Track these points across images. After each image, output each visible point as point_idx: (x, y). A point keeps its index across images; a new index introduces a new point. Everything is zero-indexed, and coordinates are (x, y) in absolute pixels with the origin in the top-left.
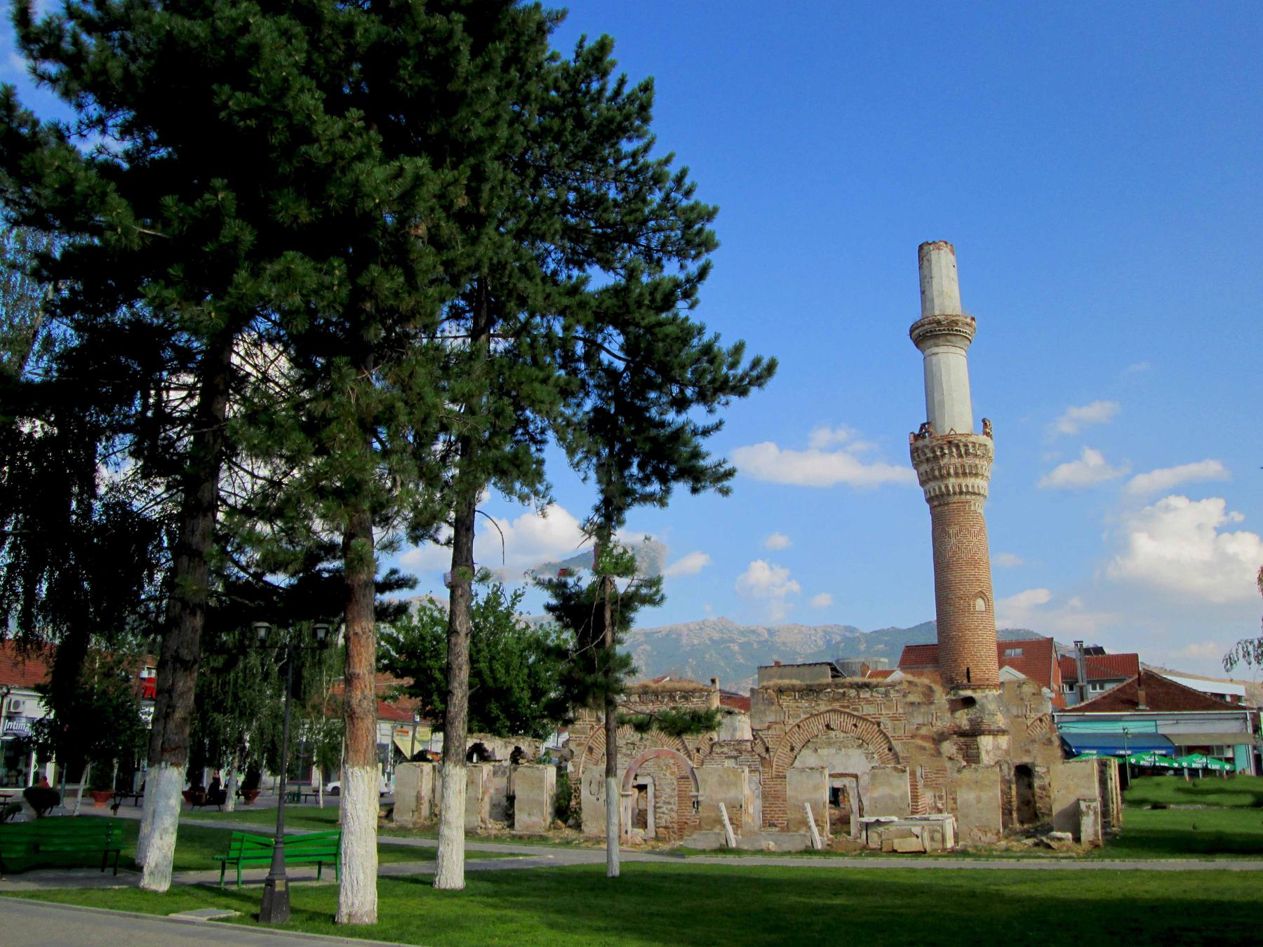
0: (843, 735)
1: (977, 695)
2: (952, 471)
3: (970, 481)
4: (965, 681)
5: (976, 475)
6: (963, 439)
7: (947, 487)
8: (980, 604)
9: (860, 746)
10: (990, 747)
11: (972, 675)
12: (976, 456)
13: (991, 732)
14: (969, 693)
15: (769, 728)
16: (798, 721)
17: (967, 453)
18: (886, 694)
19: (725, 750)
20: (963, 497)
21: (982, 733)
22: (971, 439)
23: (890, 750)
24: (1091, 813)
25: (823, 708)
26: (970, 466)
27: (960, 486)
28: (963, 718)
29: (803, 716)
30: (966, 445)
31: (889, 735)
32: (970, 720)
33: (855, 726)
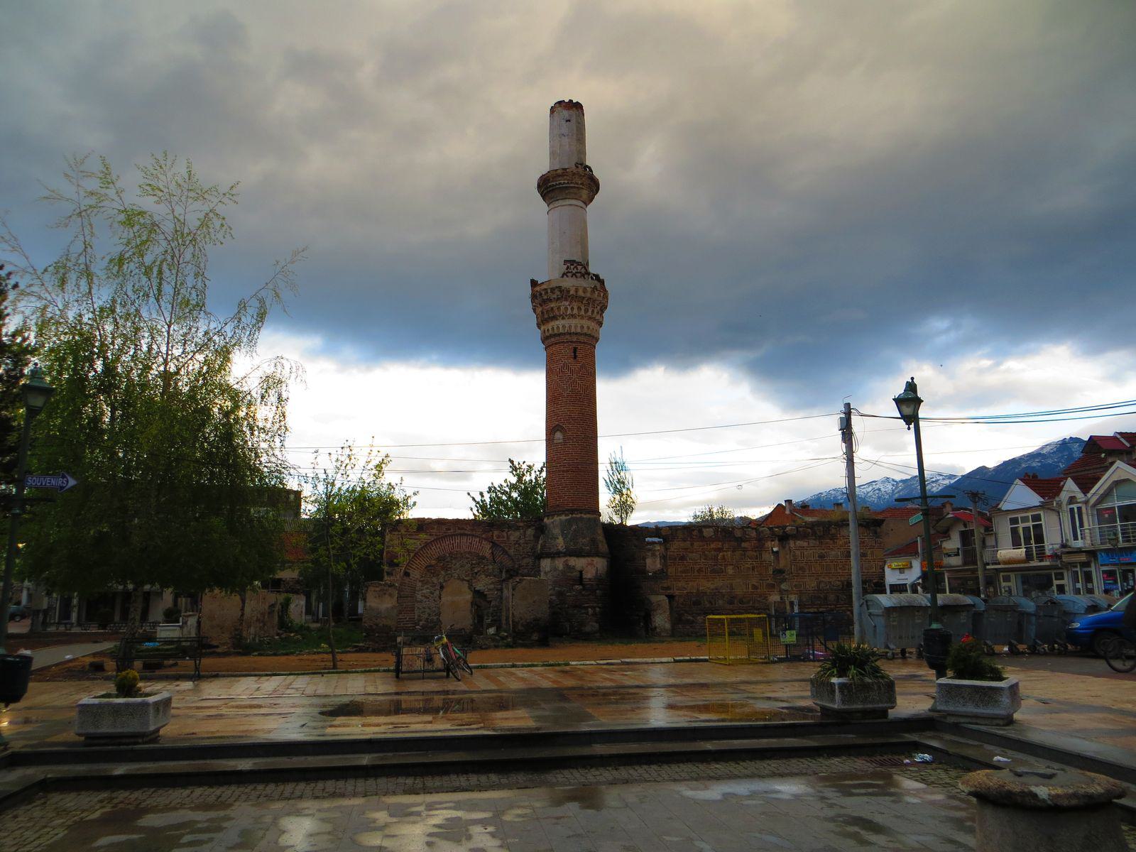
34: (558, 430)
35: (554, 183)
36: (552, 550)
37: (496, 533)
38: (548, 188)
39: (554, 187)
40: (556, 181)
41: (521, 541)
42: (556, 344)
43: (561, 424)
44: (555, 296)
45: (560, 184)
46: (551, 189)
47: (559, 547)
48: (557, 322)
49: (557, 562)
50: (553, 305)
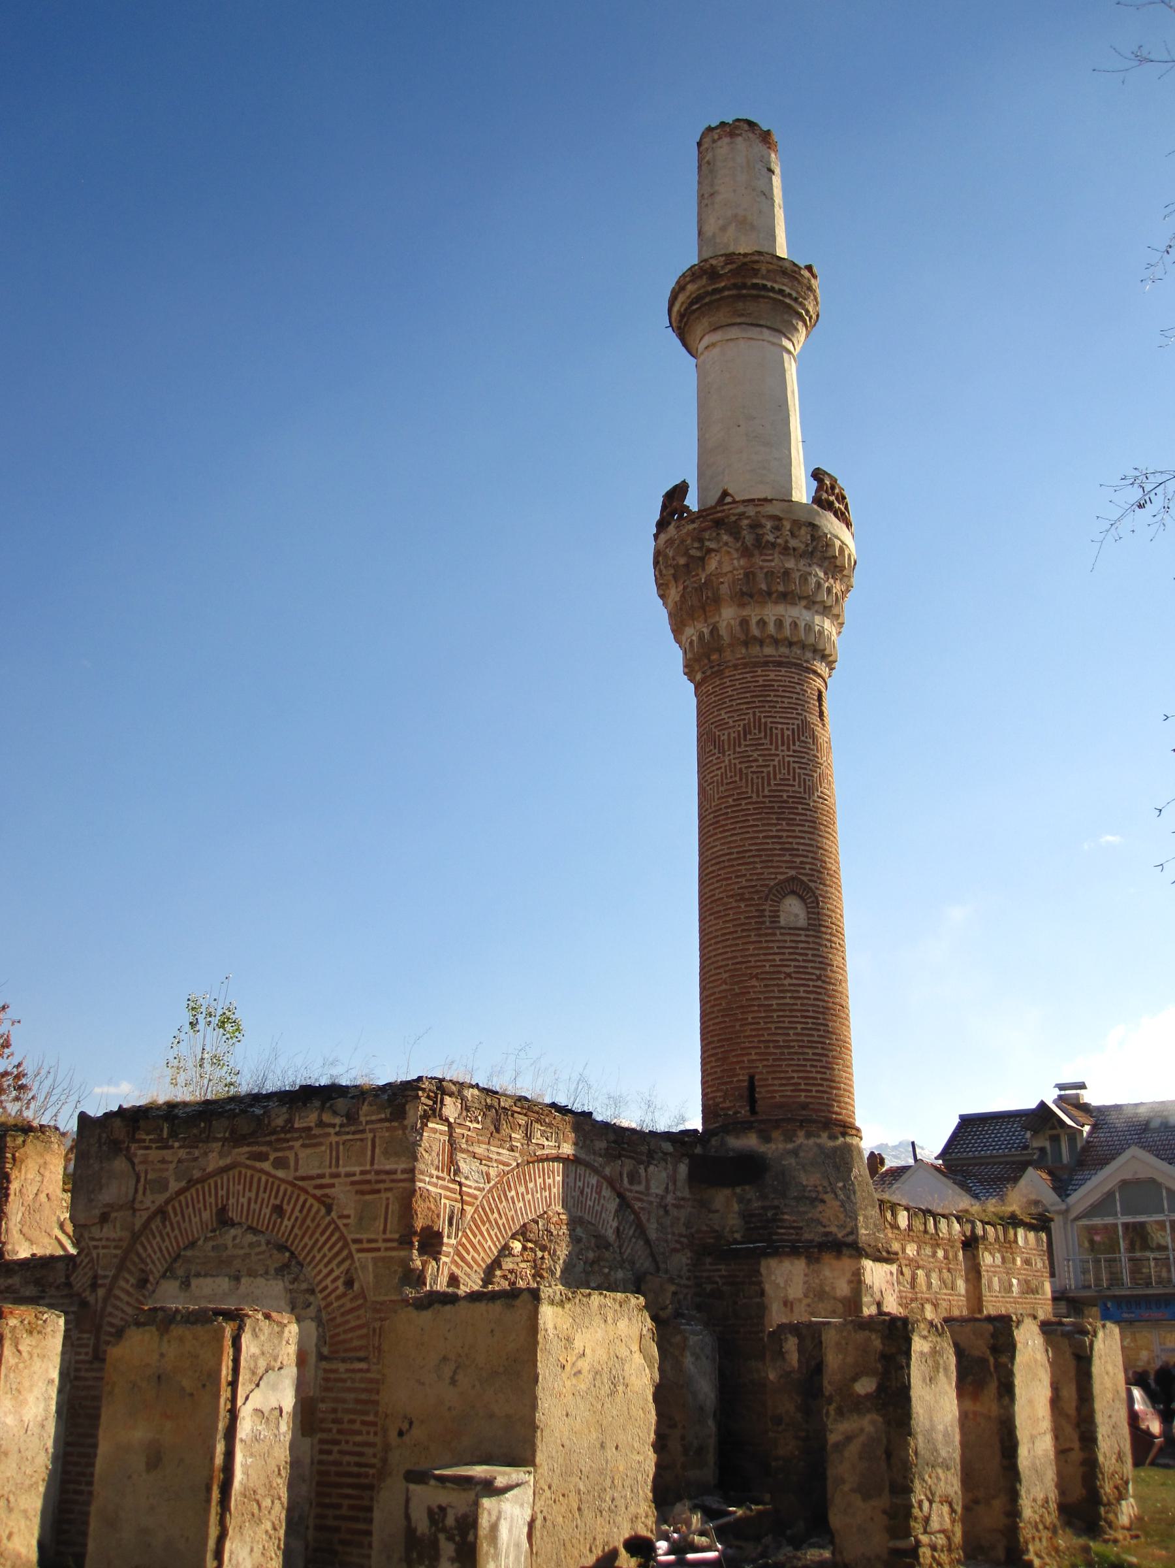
0: (250, 1238)
1: (774, 1148)
2: (724, 589)
3: (772, 612)
4: (744, 1112)
5: (786, 597)
6: (751, 511)
7: (714, 630)
8: (793, 910)
9: (282, 1270)
10: (796, 1291)
11: (760, 1093)
12: (786, 550)
13: (795, 1250)
14: (750, 1142)
15: (104, 1218)
16: (161, 1199)
17: (761, 545)
18: (352, 1117)
19: (15, 1280)
20: (755, 650)
21: (775, 1251)
22: (770, 509)
23: (349, 1283)
24: (447, 1549)
25: (214, 1161)
26: (770, 574)
27: (744, 622)
28: (728, 1208)
29: (174, 1186)
30: (755, 526)
31: (350, 1237)
32: (747, 1216)
33: (279, 1210)
34: (793, 892)
35: (769, 284)
36: (807, 1236)
37: (629, 1164)
38: (744, 286)
39: (762, 293)
40: (776, 282)
41: (670, 1199)
42: (780, 664)
43: (805, 878)
44: (793, 543)
45: (781, 292)
46: (754, 292)
47: (834, 1229)
48: (780, 609)
49: (827, 1273)
50: (790, 564)
